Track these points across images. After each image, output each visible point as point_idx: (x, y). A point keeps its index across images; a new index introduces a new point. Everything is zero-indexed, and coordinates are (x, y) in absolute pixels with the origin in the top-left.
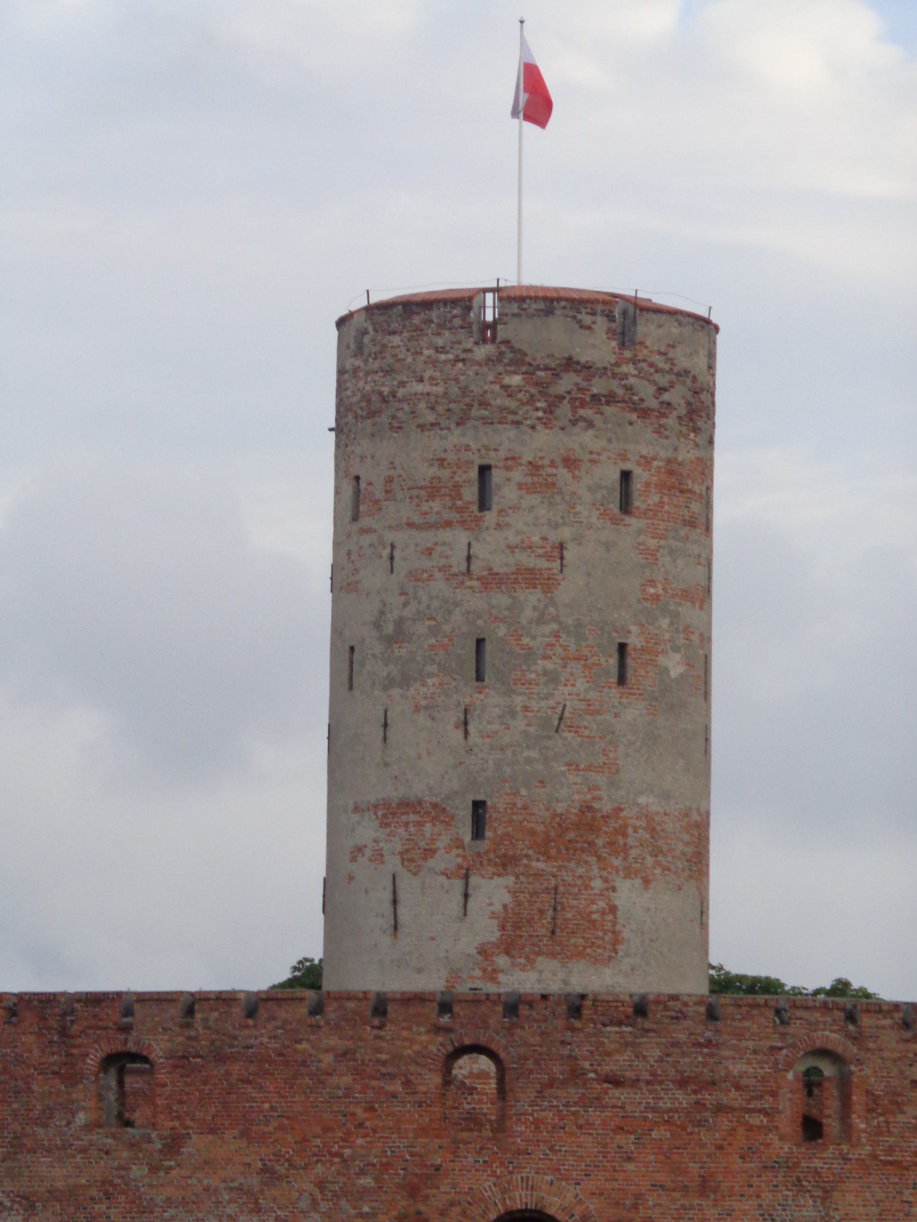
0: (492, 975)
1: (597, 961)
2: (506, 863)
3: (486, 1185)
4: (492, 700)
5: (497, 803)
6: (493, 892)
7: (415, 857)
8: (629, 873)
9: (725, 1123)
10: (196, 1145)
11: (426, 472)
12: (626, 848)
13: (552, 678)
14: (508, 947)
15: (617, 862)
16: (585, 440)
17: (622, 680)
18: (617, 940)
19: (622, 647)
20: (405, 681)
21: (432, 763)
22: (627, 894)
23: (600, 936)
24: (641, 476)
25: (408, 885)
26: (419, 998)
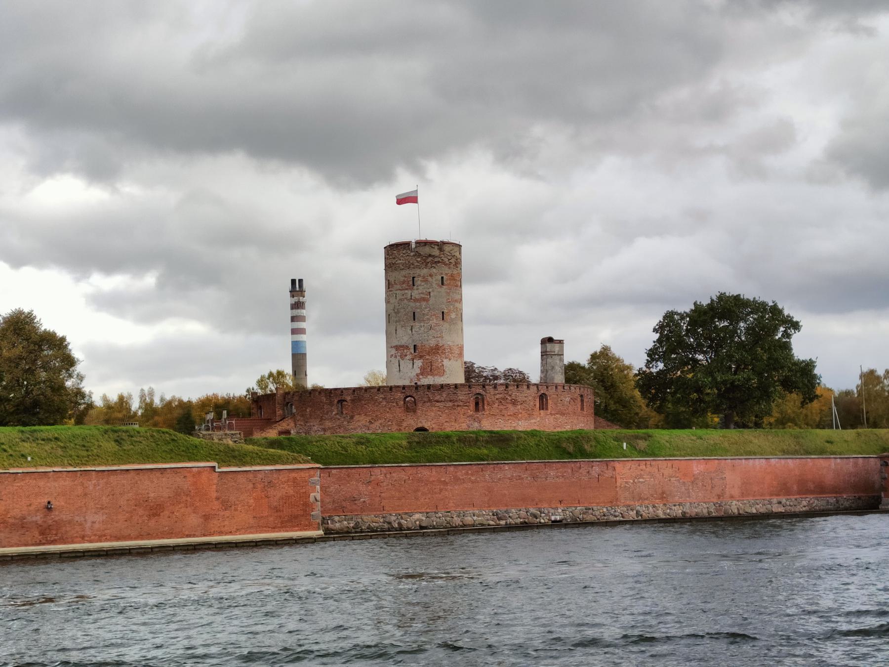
0: (419, 380)
1: (440, 376)
2: (421, 357)
3: (412, 422)
4: (417, 325)
5: (419, 345)
6: (419, 363)
7: (403, 357)
9: (459, 408)
10: (357, 417)
11: (402, 279)
13: (428, 319)
14: (422, 374)
16: (434, 270)
20: (399, 321)
21: (404, 337)
22: (446, 362)
23: (441, 372)
25: (402, 362)
26: (398, 387)
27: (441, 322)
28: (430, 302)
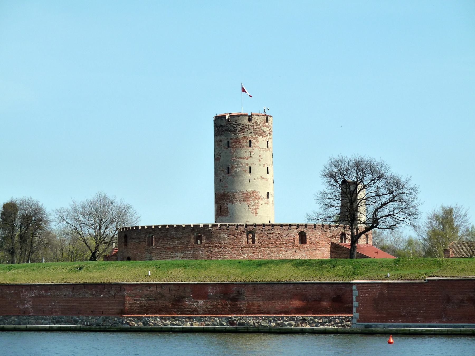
8: (230, 202)
15: (228, 201)
17: (228, 173)
18: (228, 213)
19: (228, 168)
24: (231, 141)
27: (227, 175)
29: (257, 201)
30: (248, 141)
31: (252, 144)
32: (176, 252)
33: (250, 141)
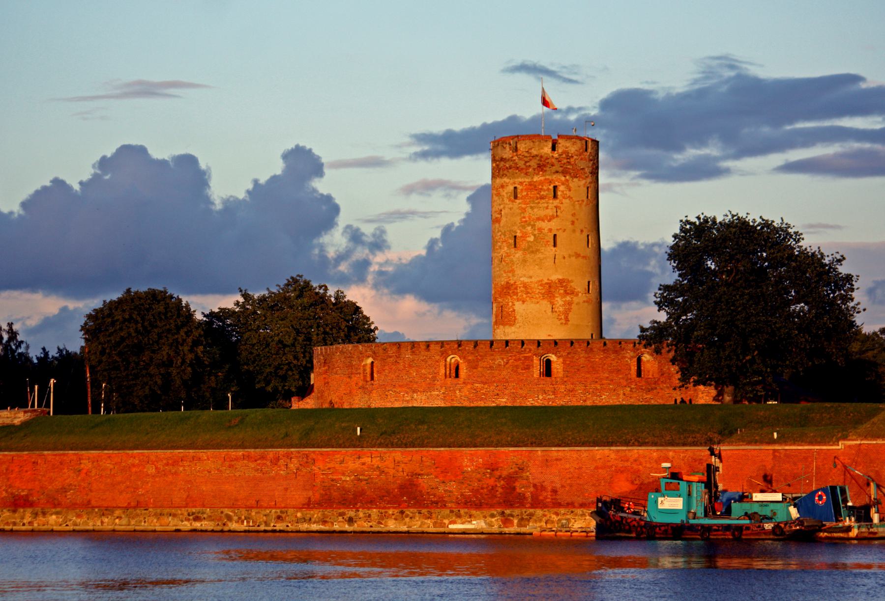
1: (511, 325)
8: (518, 300)
12: (517, 293)
16: (506, 180)
22: (518, 307)
24: (520, 187)
27: (513, 250)
28: (502, 223)
29: (568, 298)
30: (551, 187)
31: (559, 193)
32: (414, 392)
33: (555, 187)
